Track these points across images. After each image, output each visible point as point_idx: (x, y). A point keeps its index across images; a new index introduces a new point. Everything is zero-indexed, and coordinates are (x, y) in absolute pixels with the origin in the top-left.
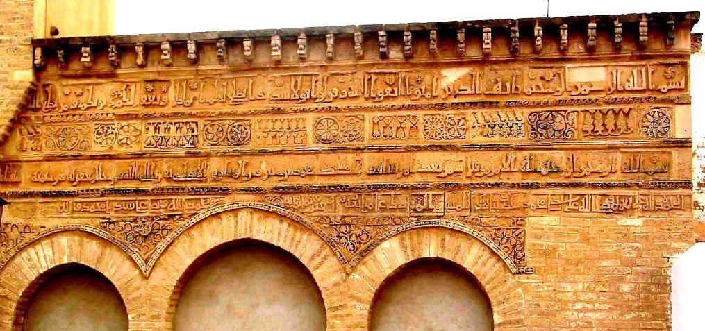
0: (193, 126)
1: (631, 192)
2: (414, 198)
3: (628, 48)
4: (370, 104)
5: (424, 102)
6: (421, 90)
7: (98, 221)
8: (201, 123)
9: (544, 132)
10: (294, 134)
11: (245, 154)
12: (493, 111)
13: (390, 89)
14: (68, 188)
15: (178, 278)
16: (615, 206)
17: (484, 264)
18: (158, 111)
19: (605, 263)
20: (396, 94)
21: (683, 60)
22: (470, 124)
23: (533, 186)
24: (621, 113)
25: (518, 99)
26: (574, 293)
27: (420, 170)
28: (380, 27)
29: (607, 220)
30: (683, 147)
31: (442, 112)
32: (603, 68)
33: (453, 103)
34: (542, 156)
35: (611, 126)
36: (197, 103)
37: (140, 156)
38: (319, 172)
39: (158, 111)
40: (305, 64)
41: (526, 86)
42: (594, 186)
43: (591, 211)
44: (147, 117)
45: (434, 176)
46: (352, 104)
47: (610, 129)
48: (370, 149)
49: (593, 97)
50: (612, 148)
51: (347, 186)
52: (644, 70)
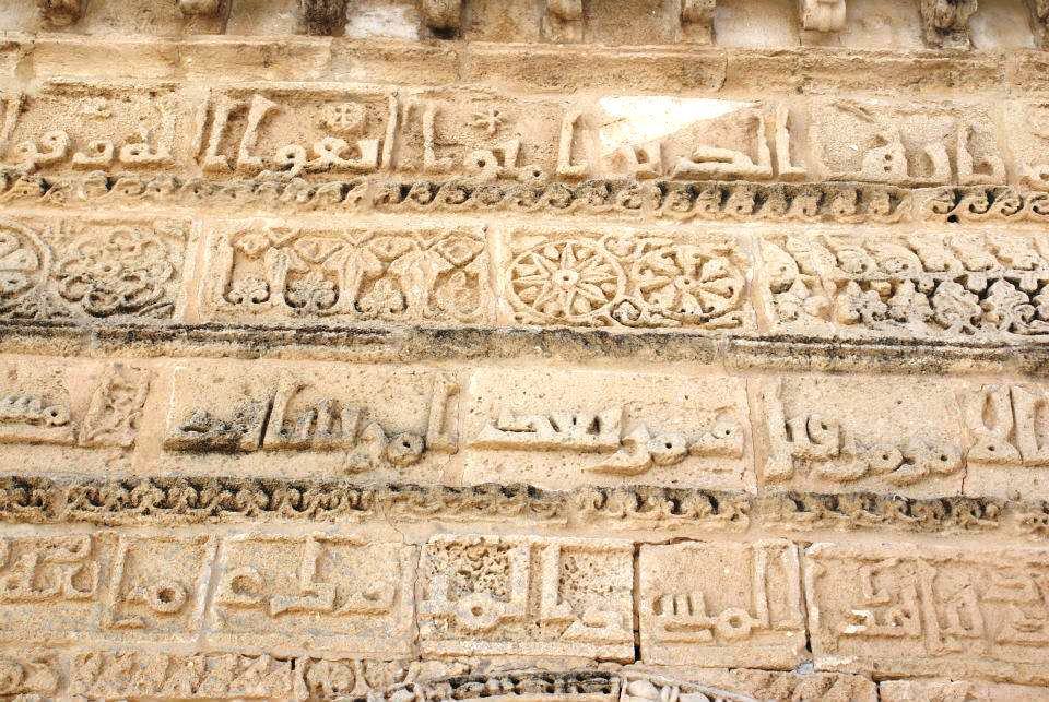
6: (499, 156)
12: (872, 231)
27: (492, 435)
31: (608, 227)
48: (200, 339)
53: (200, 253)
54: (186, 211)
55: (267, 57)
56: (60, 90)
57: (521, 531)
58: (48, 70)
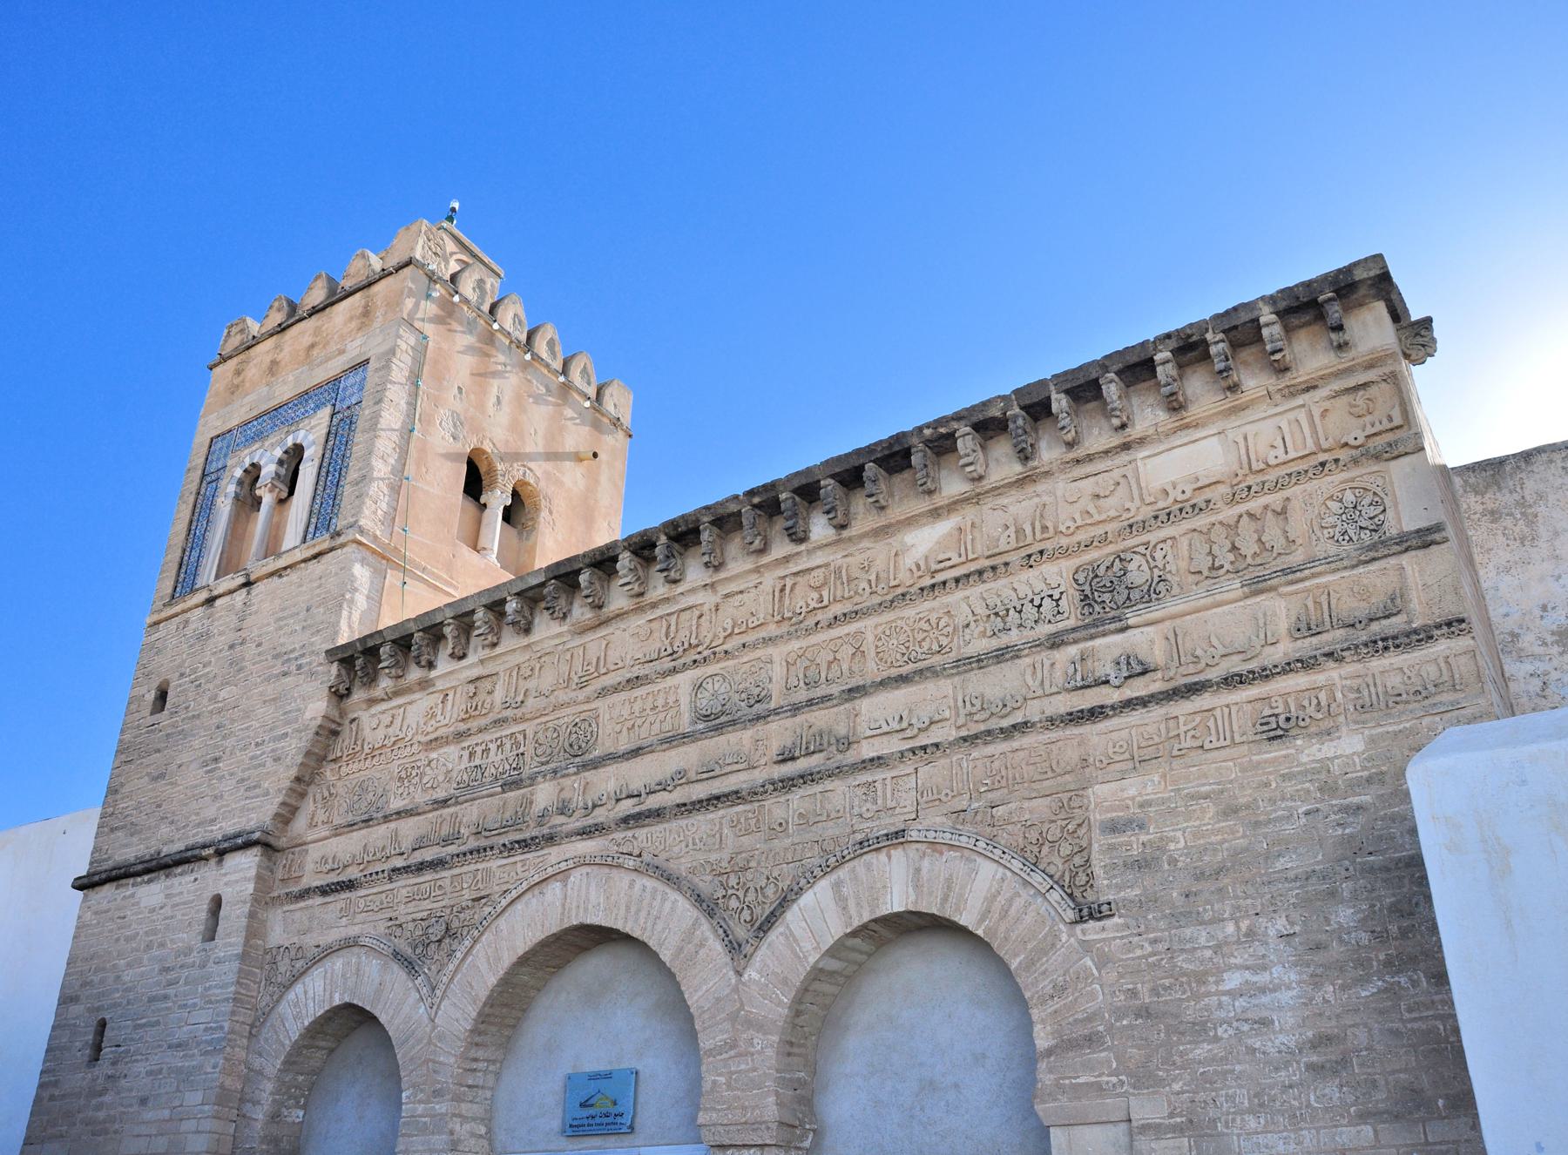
0: (520, 738)
1: (1319, 678)
2: (860, 791)
3: (1254, 382)
4: (785, 628)
5: (876, 600)
7: (382, 927)
8: (530, 733)
9: (1107, 597)
10: (662, 716)
11: (585, 767)
12: (1002, 582)
13: (815, 595)
14: (353, 873)
15: (474, 1014)
16: (1288, 719)
17: (1004, 913)
18: (474, 725)
19: (1280, 864)
20: (826, 602)
21: (1387, 370)
22: (960, 621)
23: (1095, 714)
24: (1269, 514)
25: (1047, 545)
26: (1217, 949)
28: (772, 487)
29: (1276, 751)
30: (1426, 546)
32: (1215, 439)
33: (922, 589)
34: (1109, 646)
35: (1249, 547)
36: (530, 702)
37: (444, 803)
38: (692, 775)
39: (474, 725)
40: (680, 590)
41: (1065, 517)
42: (1233, 681)
43: (1234, 743)
44: (460, 736)
45: (896, 738)
46: (749, 638)
47: (1249, 553)
49: (1199, 499)
50: (1257, 587)
51: (737, 792)
52: (1302, 415)
53: (775, 668)
54: (770, 650)
55: (787, 559)
56: (727, 596)
57: (878, 775)
58: (723, 590)
